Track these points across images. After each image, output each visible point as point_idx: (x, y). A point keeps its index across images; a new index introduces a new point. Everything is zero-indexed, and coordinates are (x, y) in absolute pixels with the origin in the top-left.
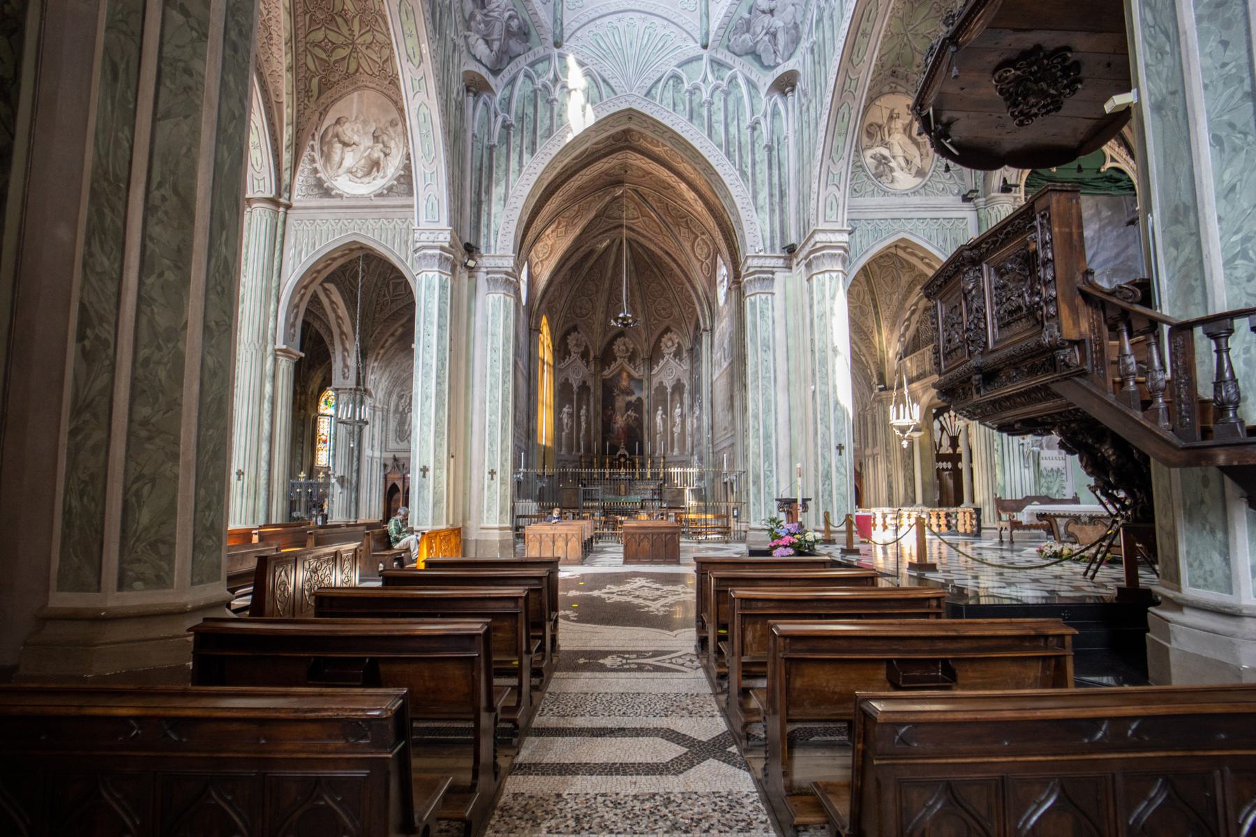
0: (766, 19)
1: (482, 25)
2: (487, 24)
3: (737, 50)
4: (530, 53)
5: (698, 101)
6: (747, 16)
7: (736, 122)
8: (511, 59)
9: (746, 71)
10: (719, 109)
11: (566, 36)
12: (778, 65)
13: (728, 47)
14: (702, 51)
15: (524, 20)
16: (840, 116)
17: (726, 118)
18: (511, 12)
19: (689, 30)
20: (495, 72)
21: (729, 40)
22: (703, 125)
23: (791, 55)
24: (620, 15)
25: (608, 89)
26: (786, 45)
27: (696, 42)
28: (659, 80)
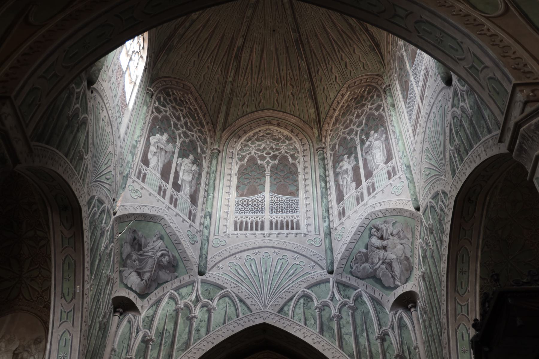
0: (382, 253)
1: (137, 262)
2: (140, 261)
3: (359, 274)
4: (176, 280)
5: (327, 316)
7: (365, 334)
8: (159, 285)
9: (369, 291)
10: (348, 323)
11: (209, 266)
12: (397, 286)
13: (351, 273)
14: (329, 276)
15: (174, 257)
16: (459, 335)
17: (355, 330)
18: (163, 252)
19: (316, 260)
20: (142, 296)
21: (352, 268)
22: (333, 337)
23: (407, 281)
24: (257, 250)
25: (244, 307)
26: (401, 272)
27: (324, 269)
28: (291, 299)
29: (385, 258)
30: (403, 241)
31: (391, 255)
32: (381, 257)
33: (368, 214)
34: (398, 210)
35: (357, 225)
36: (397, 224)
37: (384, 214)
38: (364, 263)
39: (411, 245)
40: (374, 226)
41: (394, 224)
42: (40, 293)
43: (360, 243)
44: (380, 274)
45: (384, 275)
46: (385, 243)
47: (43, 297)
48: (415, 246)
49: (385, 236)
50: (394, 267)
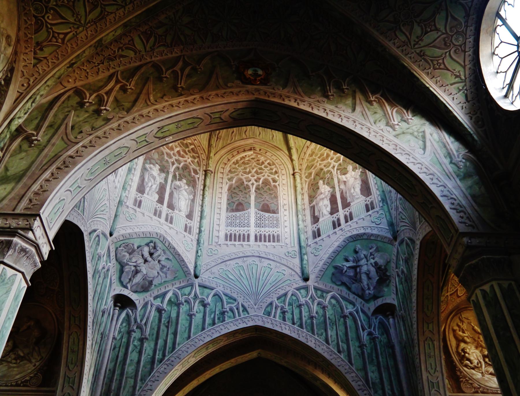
0: (141, 261)
3: (118, 255)
6: (136, 248)
13: (117, 249)
21: (120, 247)
23: (135, 292)
26: (138, 284)
29: (139, 265)
30: (161, 273)
31: (144, 269)
32: (138, 262)
33: (160, 234)
34: (181, 258)
35: (148, 230)
36: (170, 262)
37: (169, 247)
38: (128, 252)
39: (164, 282)
40: (155, 243)
41: (168, 259)
42: (50, 5)
43: (139, 240)
44: (127, 269)
45: (127, 272)
46: (149, 259)
47: (47, 12)
48: (166, 285)
49: (155, 255)
50: (137, 276)
